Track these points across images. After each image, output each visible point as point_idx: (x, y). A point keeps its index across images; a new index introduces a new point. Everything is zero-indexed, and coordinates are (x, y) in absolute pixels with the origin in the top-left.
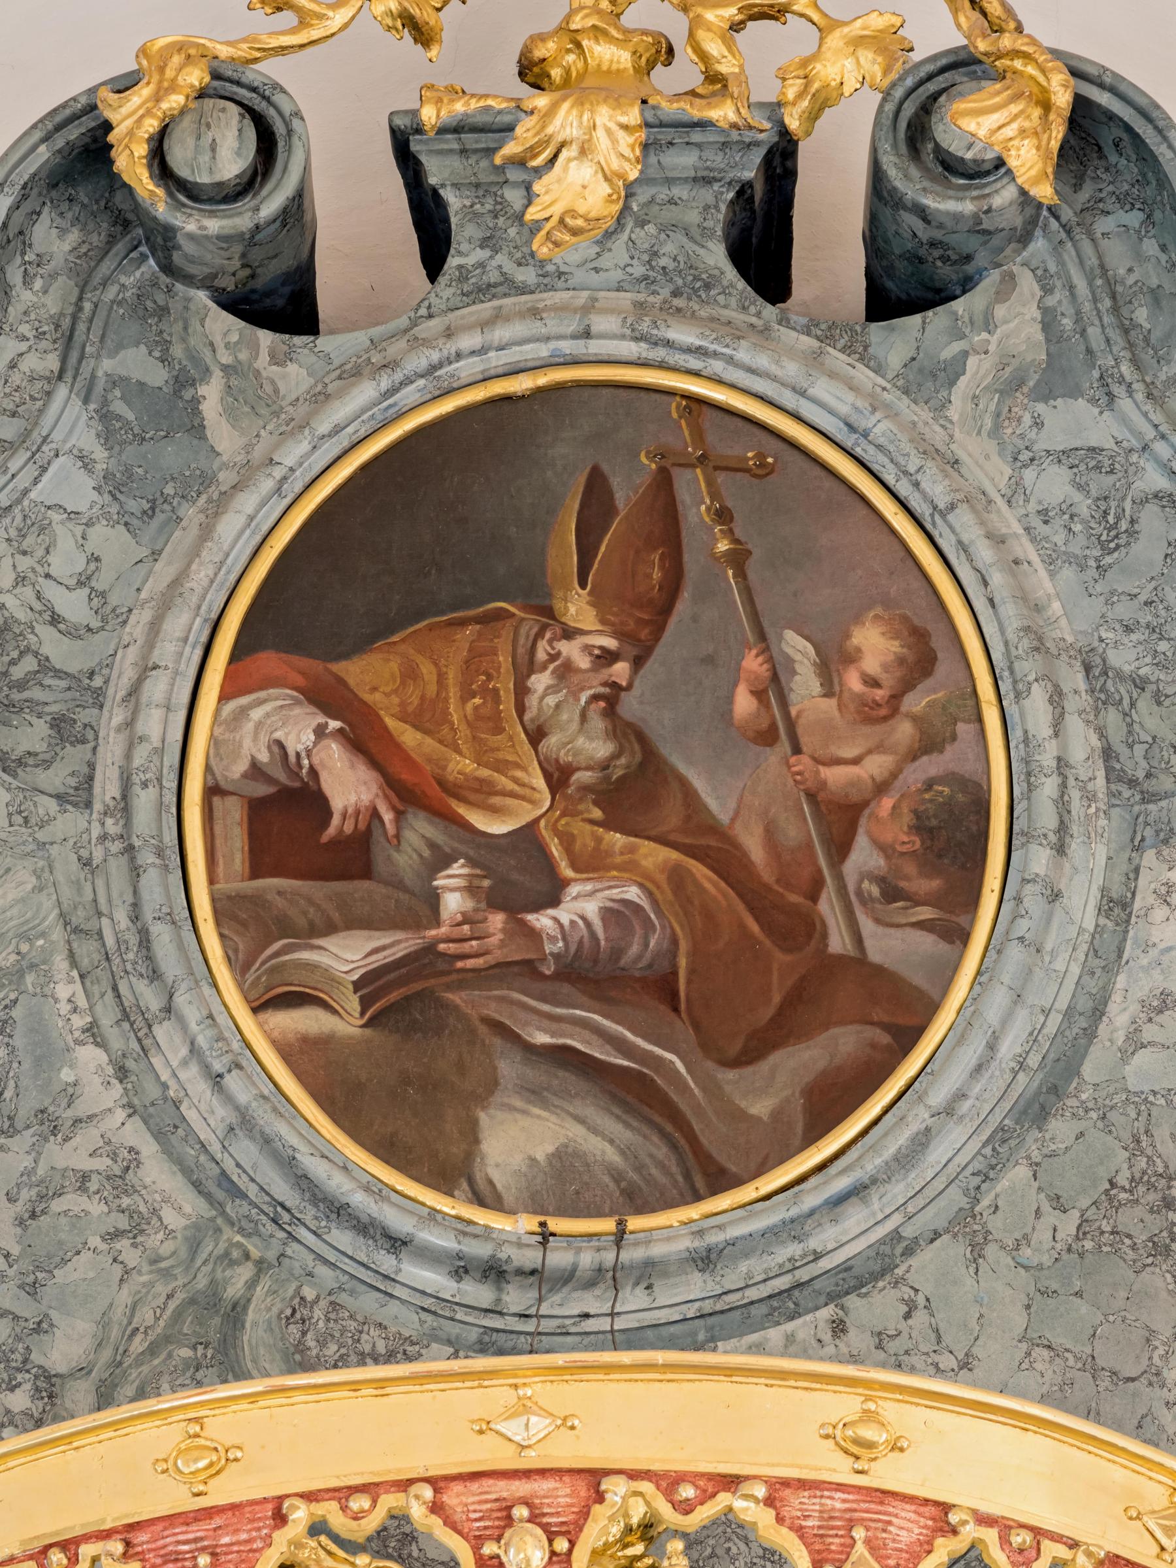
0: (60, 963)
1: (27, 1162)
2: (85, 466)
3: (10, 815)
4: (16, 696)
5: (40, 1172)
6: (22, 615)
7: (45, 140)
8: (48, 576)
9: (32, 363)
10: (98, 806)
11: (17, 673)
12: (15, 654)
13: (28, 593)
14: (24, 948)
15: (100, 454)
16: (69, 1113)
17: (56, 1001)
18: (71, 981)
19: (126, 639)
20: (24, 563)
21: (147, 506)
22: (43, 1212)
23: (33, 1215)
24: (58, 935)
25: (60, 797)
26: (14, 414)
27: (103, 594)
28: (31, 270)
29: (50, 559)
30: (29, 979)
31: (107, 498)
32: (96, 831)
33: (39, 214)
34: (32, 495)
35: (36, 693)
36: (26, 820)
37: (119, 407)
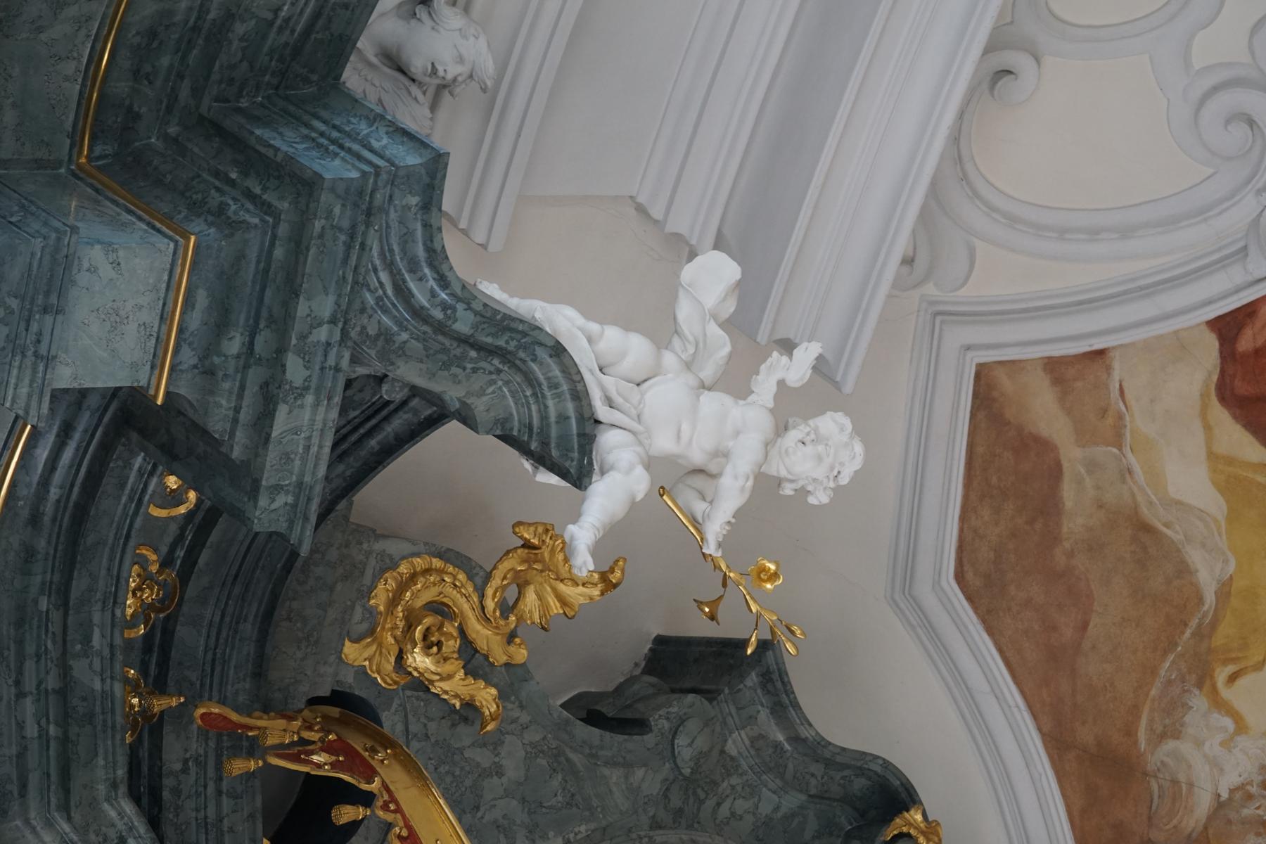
0: (592, 826)
1: (518, 822)
2: (775, 809)
3: (648, 796)
4: (690, 792)
5: (514, 828)
6: (720, 790)
7: (902, 784)
8: (735, 799)
9: (813, 782)
10: (651, 833)
11: (699, 791)
12: (706, 789)
13: (728, 792)
14: (599, 810)
15: (779, 815)
16: (537, 836)
17: (579, 826)
18: (587, 831)
19: (713, 836)
20: (739, 788)
21: (761, 837)
22: (499, 831)
23: (498, 827)
24: (604, 823)
25: (653, 817)
26: (794, 777)
27: (728, 823)
28: (848, 779)
29: (741, 799)
30: (587, 813)
31: (763, 820)
32: (642, 833)
33: (870, 780)
34: (764, 789)
35: (691, 801)
36: (646, 803)
37: (796, 821)
